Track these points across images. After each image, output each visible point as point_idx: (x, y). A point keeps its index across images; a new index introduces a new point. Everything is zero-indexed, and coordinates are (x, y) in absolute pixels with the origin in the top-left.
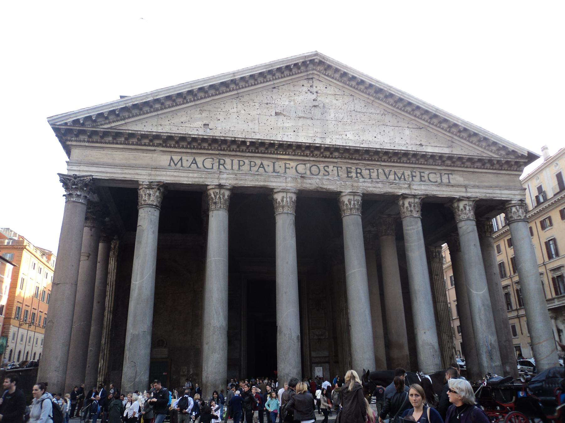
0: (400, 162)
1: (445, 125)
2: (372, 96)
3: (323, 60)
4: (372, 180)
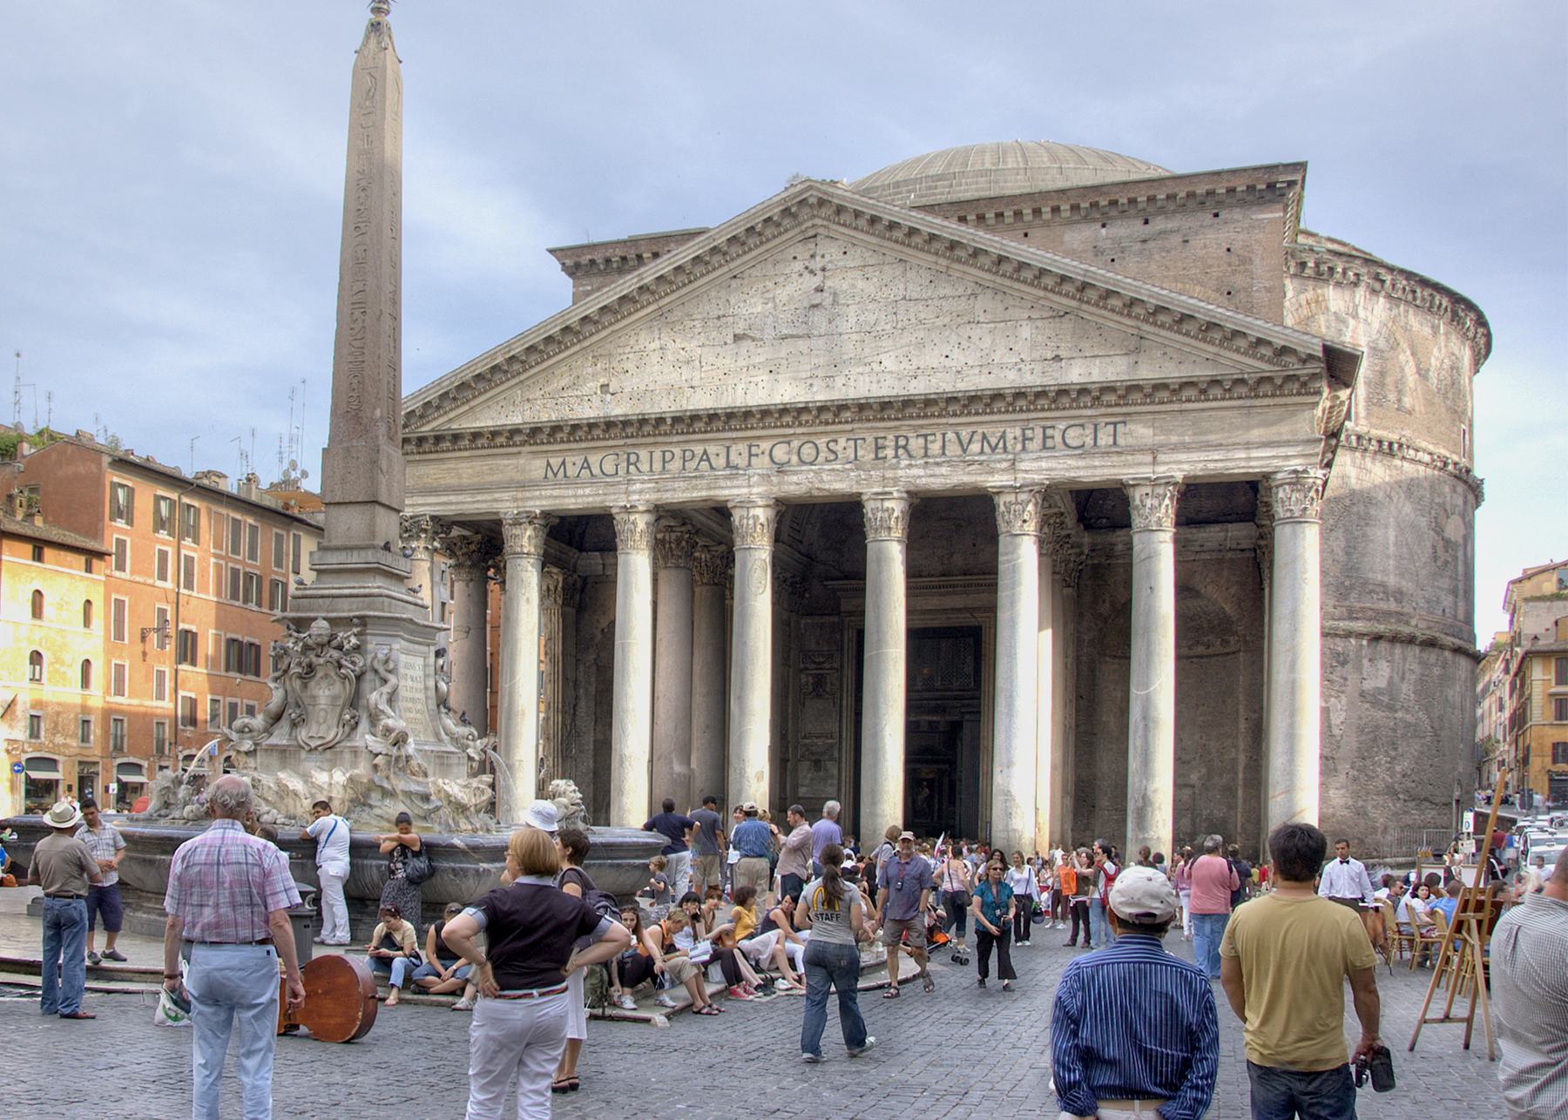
0: (992, 413)
1: (1113, 302)
2: (945, 257)
3: (825, 197)
4: (926, 460)
